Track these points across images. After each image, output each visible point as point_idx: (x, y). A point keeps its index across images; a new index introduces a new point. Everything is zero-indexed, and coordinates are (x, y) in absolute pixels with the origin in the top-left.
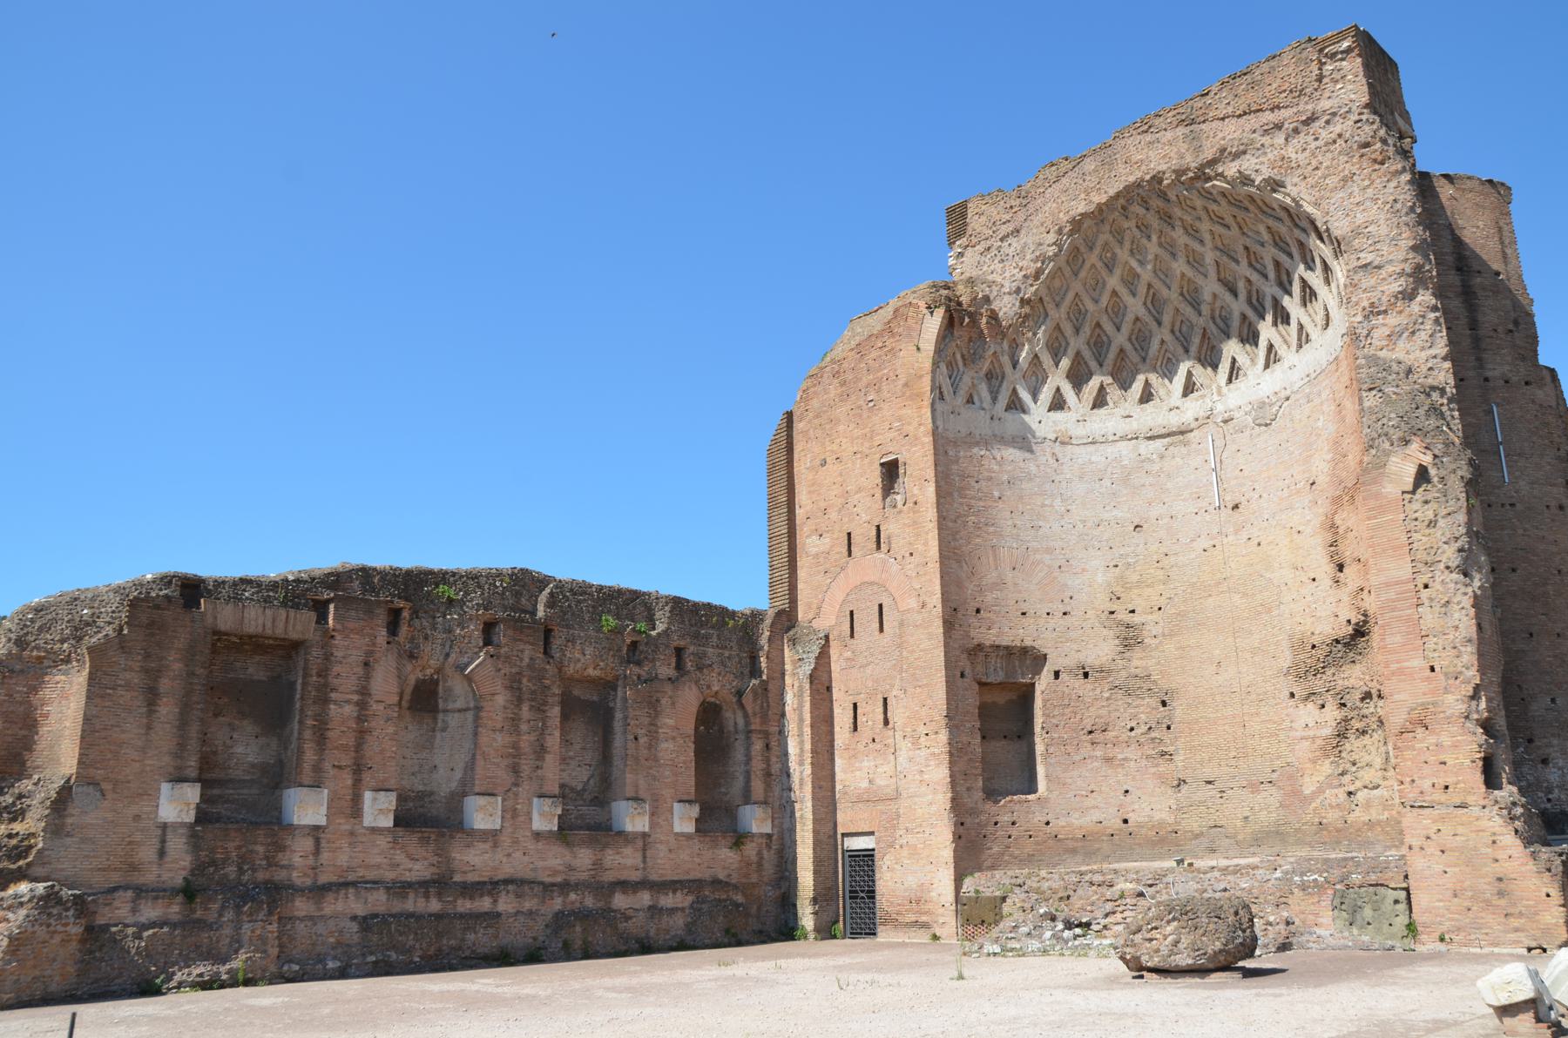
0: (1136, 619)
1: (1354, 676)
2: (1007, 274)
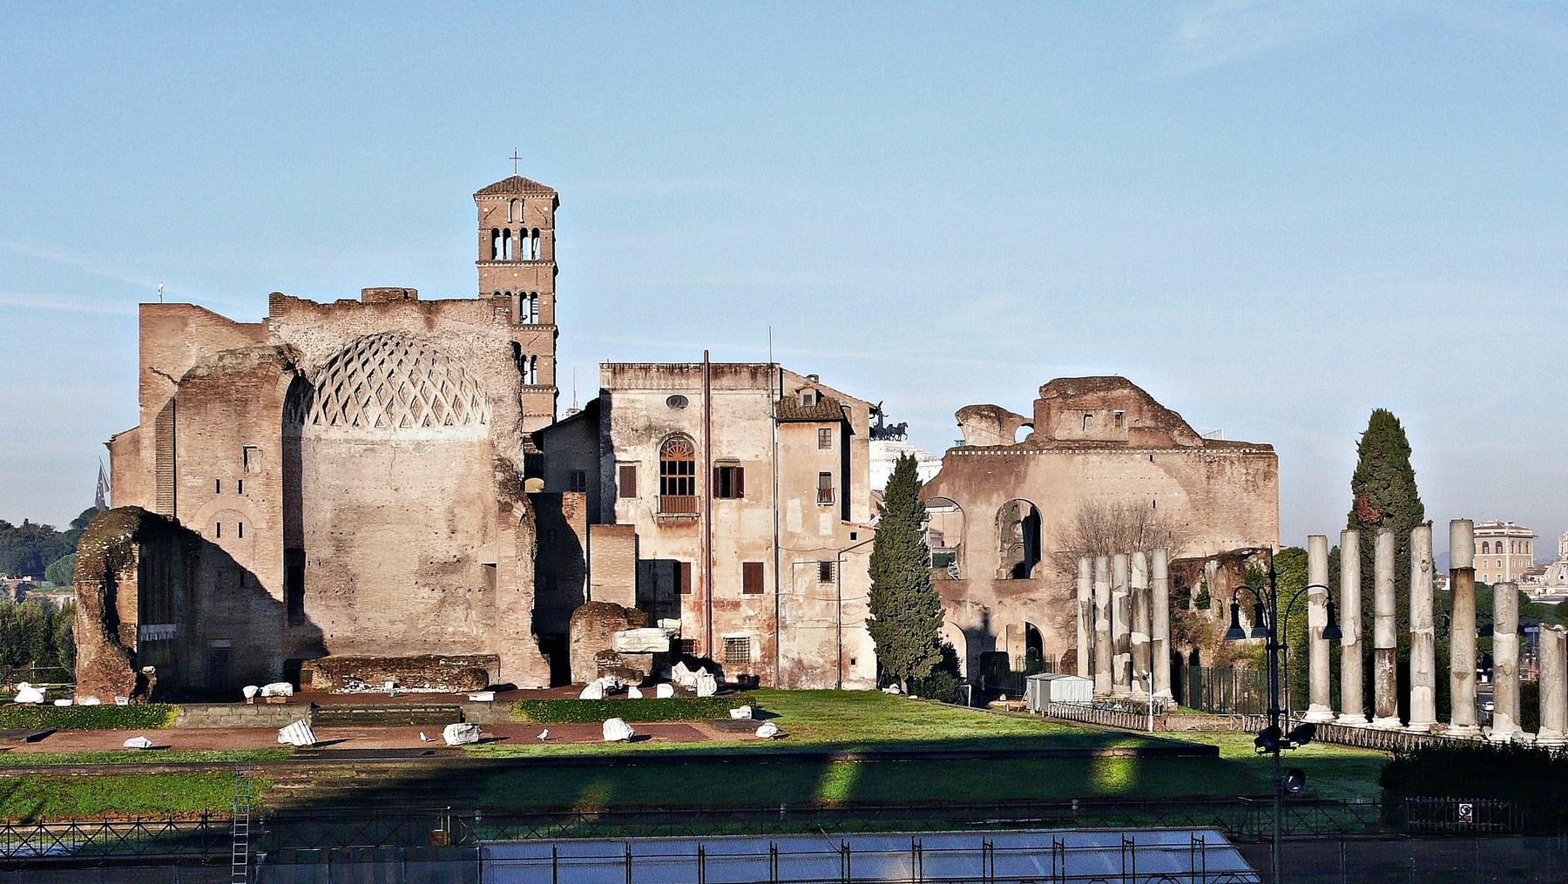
0: (342, 537)
1: (453, 579)
2: (309, 349)
